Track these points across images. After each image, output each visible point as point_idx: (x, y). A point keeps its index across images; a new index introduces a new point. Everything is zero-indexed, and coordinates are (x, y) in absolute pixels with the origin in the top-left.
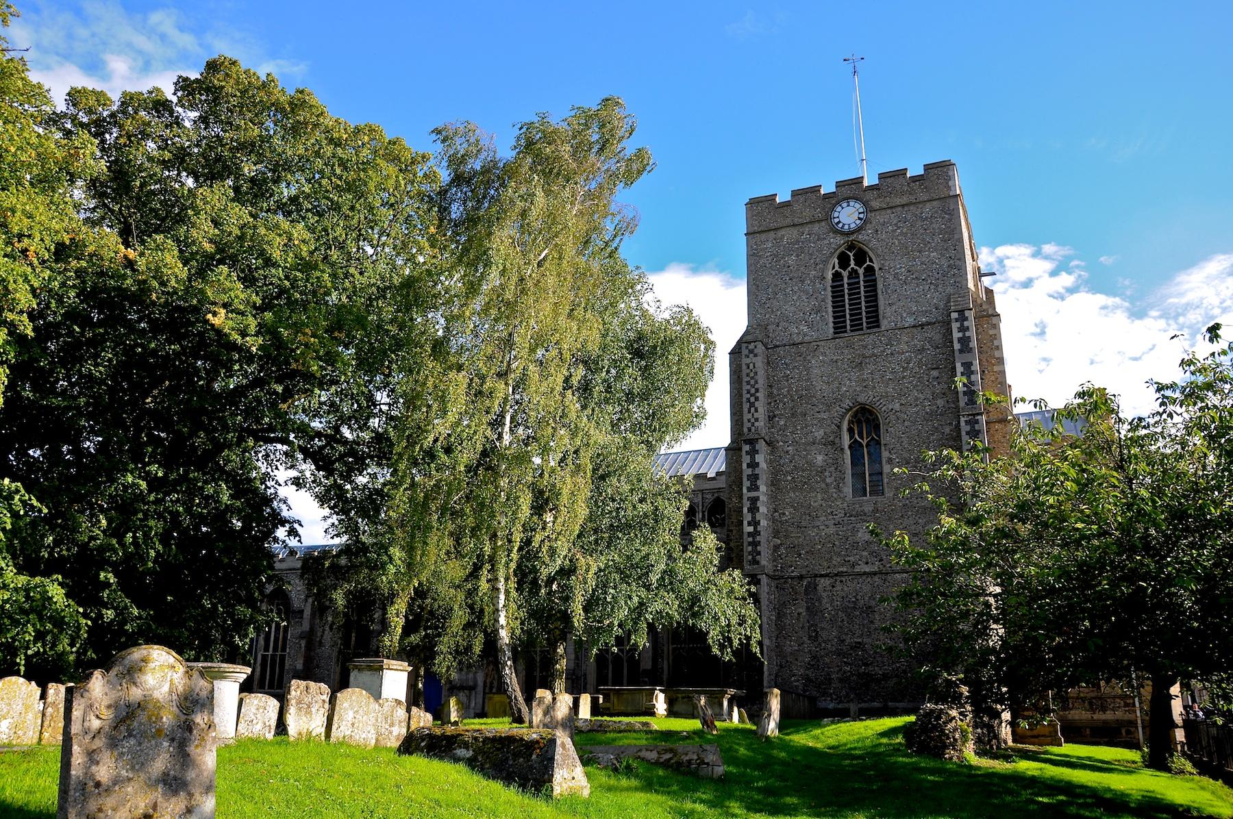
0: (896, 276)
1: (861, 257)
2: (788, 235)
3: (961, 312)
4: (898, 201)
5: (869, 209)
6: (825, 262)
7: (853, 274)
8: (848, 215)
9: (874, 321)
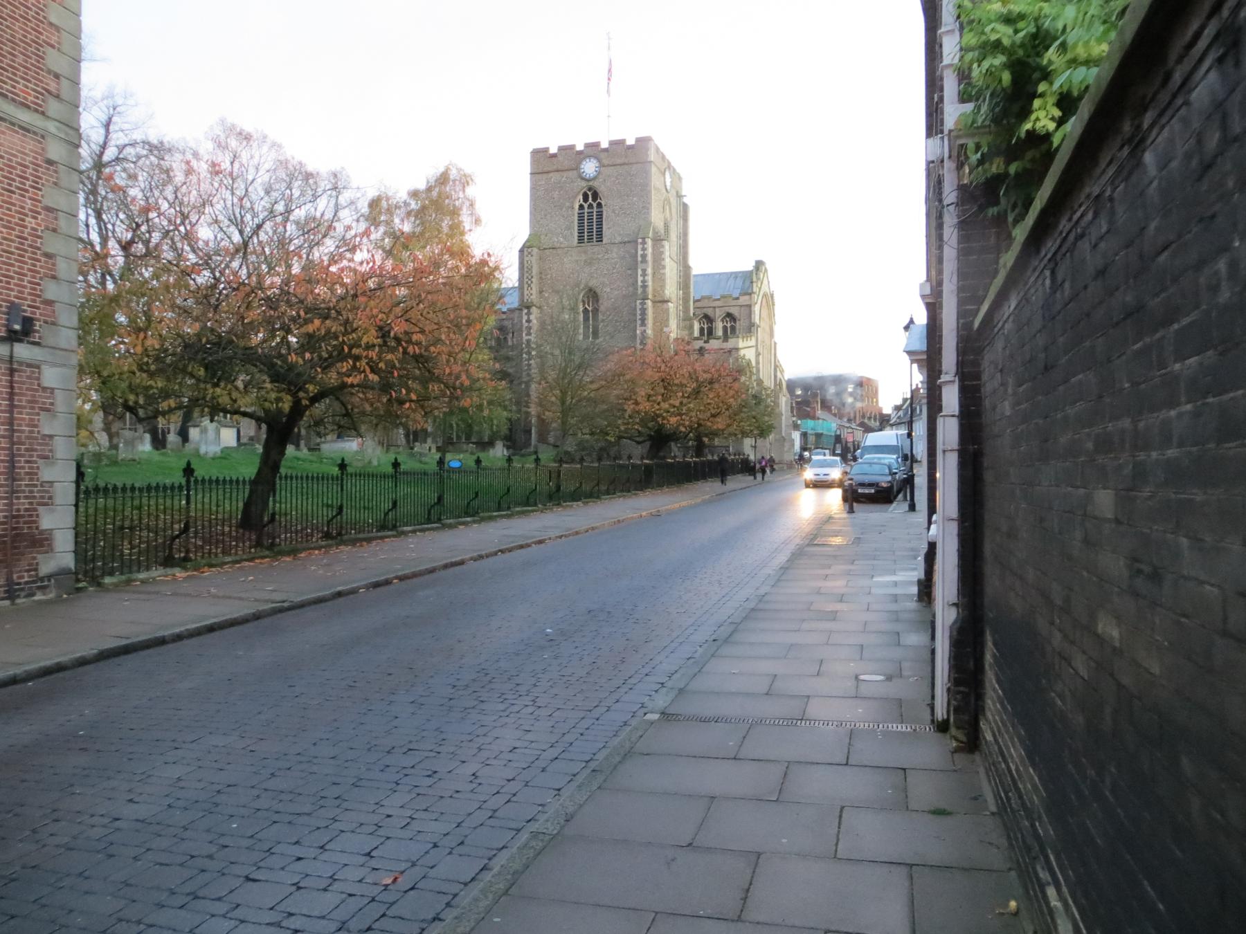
0: (614, 211)
1: (595, 196)
2: (555, 177)
3: (644, 239)
4: (619, 161)
5: (602, 165)
6: (575, 197)
7: (590, 206)
8: (589, 168)
9: (600, 239)
